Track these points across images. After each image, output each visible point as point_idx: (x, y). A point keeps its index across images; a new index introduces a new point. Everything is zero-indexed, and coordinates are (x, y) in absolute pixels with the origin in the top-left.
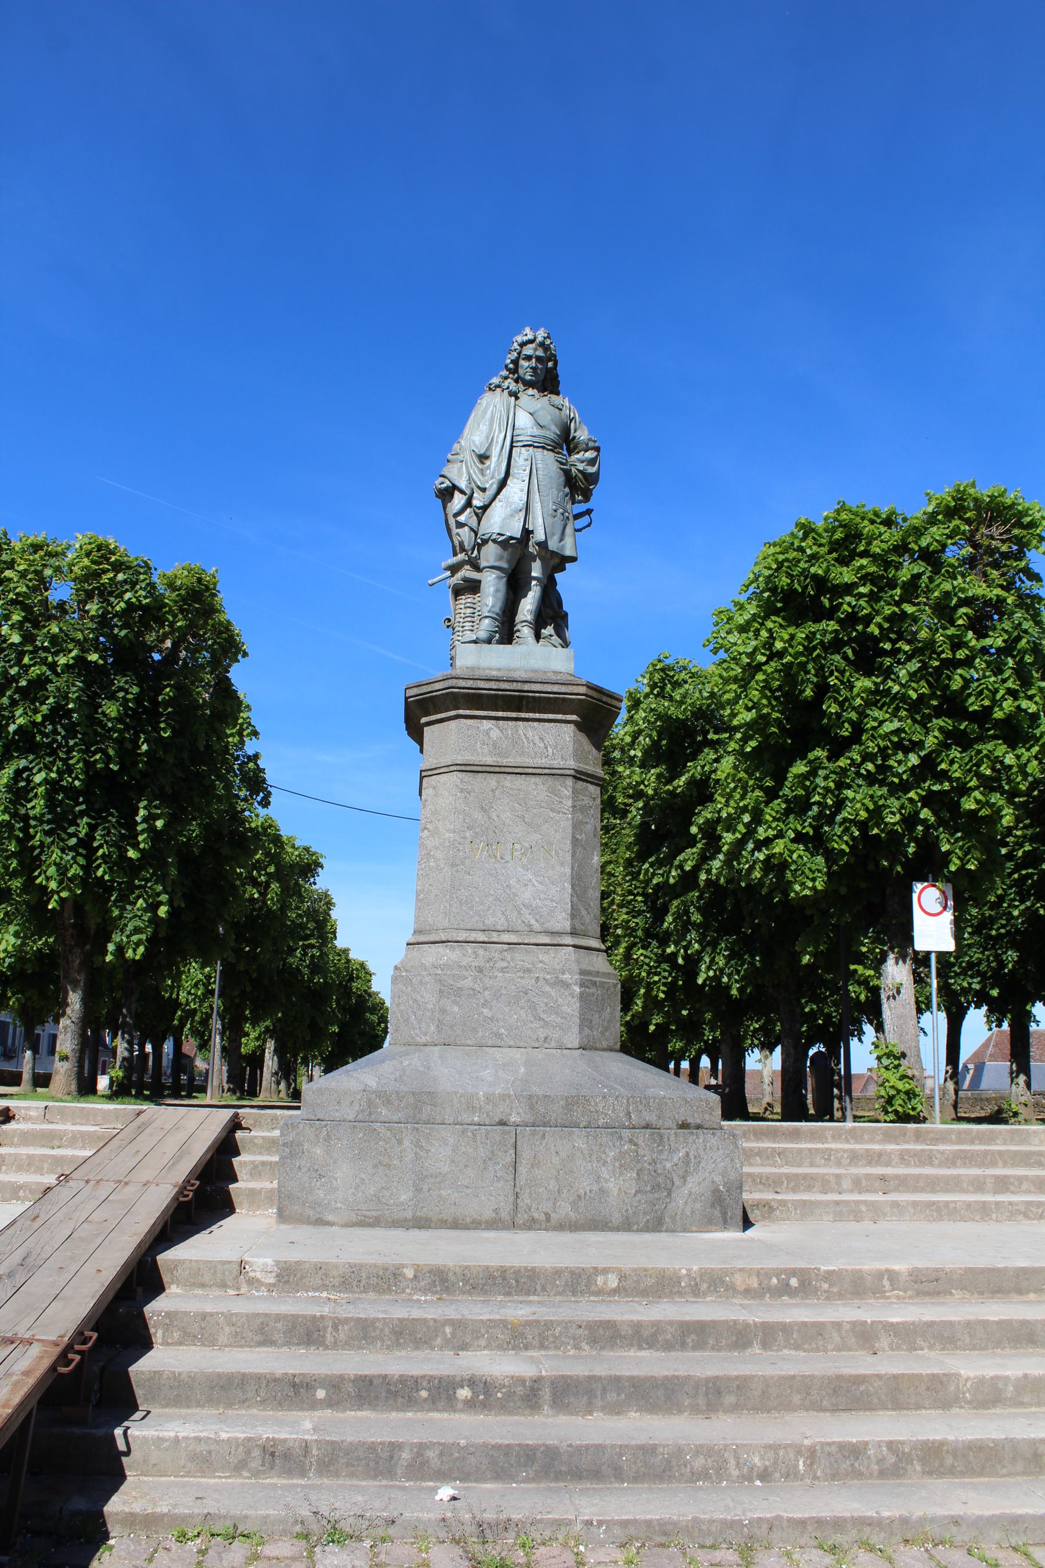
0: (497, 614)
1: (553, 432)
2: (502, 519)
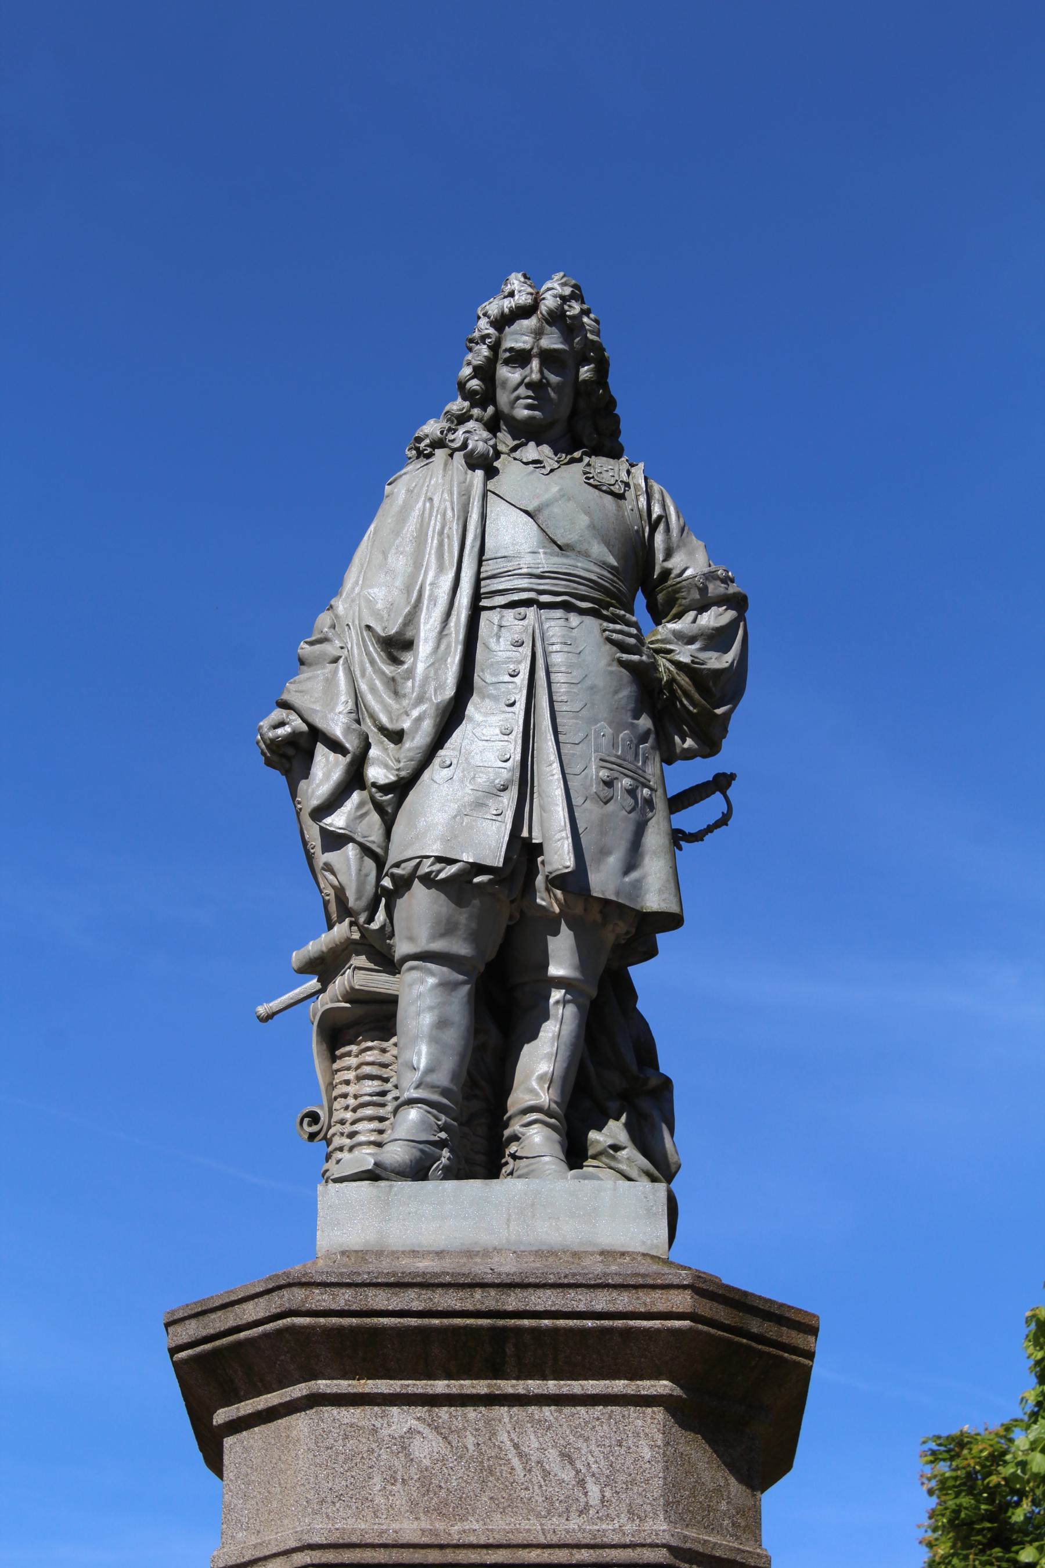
0: (445, 1092)
1: (597, 559)
2: (455, 817)
